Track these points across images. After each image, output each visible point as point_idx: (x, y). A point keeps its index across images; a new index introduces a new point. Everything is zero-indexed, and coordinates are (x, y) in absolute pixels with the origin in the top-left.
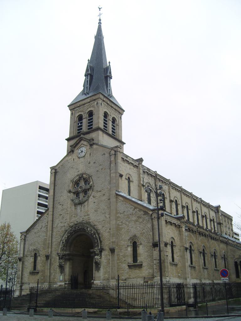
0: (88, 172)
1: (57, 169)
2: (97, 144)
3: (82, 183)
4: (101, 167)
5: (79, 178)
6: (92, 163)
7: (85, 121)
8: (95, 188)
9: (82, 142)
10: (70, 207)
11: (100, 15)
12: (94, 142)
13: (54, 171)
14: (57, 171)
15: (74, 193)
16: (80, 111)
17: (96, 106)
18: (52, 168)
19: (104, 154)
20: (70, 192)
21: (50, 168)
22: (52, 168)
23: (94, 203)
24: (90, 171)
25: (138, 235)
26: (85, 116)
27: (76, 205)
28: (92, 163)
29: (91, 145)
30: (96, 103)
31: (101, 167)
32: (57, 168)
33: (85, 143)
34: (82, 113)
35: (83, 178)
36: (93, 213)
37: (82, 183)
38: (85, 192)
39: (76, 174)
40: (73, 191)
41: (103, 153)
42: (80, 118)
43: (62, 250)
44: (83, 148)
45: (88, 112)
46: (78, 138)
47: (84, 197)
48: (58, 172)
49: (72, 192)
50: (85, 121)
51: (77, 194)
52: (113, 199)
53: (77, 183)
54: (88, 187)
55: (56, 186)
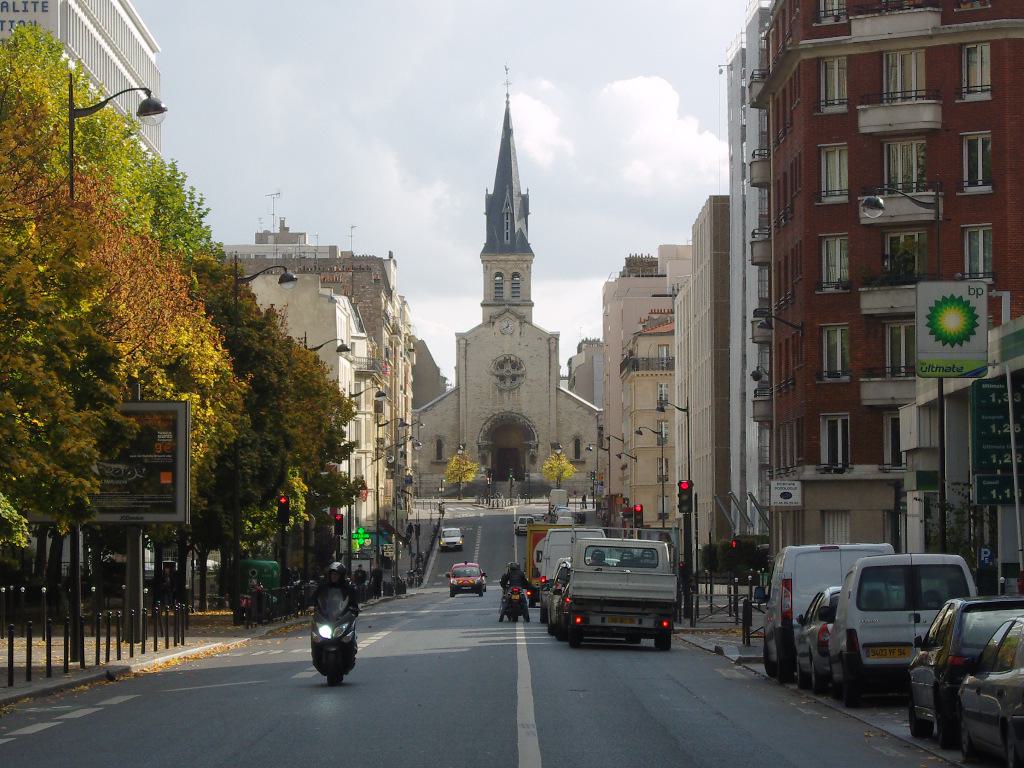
0: (518, 354)
2: (530, 323)
3: (508, 367)
7: (507, 286)
8: (529, 376)
9: (507, 314)
11: (508, 84)
13: (463, 342)
18: (460, 337)
20: (493, 374)
21: (457, 335)
22: (460, 337)
25: (582, 433)
26: (508, 277)
27: (501, 390)
29: (521, 323)
32: (468, 337)
33: (512, 317)
36: (527, 402)
37: (508, 367)
38: (514, 378)
39: (500, 353)
43: (484, 438)
46: (502, 308)
50: (507, 286)
51: (502, 378)
52: (553, 393)
53: (501, 365)
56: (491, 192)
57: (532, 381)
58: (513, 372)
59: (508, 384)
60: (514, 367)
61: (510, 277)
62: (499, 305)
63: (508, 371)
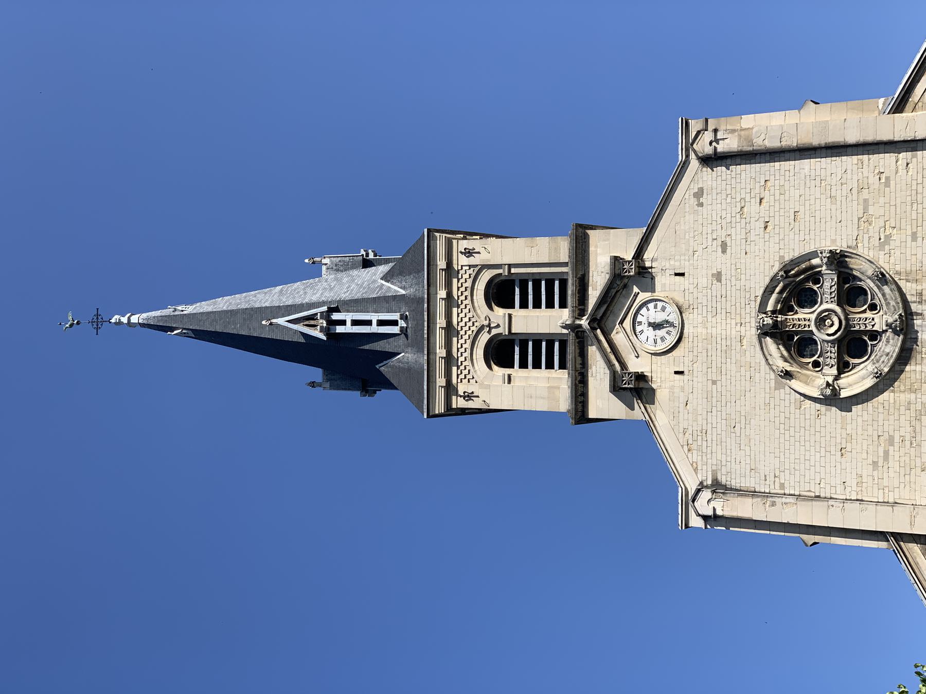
1: (701, 483)
3: (804, 317)
4: (752, 208)
5: (772, 336)
6: (721, 262)
10: (912, 390)
12: (629, 256)
14: (709, 482)
15: (843, 367)
16: (467, 354)
17: (476, 260)
19: (699, 194)
23: (914, 237)
24: (760, 268)
28: (721, 262)
30: (464, 260)
31: (752, 208)
34: (484, 338)
35: (782, 312)
40: (834, 371)
41: (693, 201)
42: (502, 352)
44: (639, 318)
45: (491, 308)
47: (873, 307)
48: (714, 473)
49: (837, 378)
51: (853, 345)
54: (829, 282)
55: (782, 486)
56: (316, 374)
57: (865, 219)
58: (828, 303)
59: (879, 321)
60: (808, 298)
61: (500, 313)
62: (583, 354)
63: (821, 321)
